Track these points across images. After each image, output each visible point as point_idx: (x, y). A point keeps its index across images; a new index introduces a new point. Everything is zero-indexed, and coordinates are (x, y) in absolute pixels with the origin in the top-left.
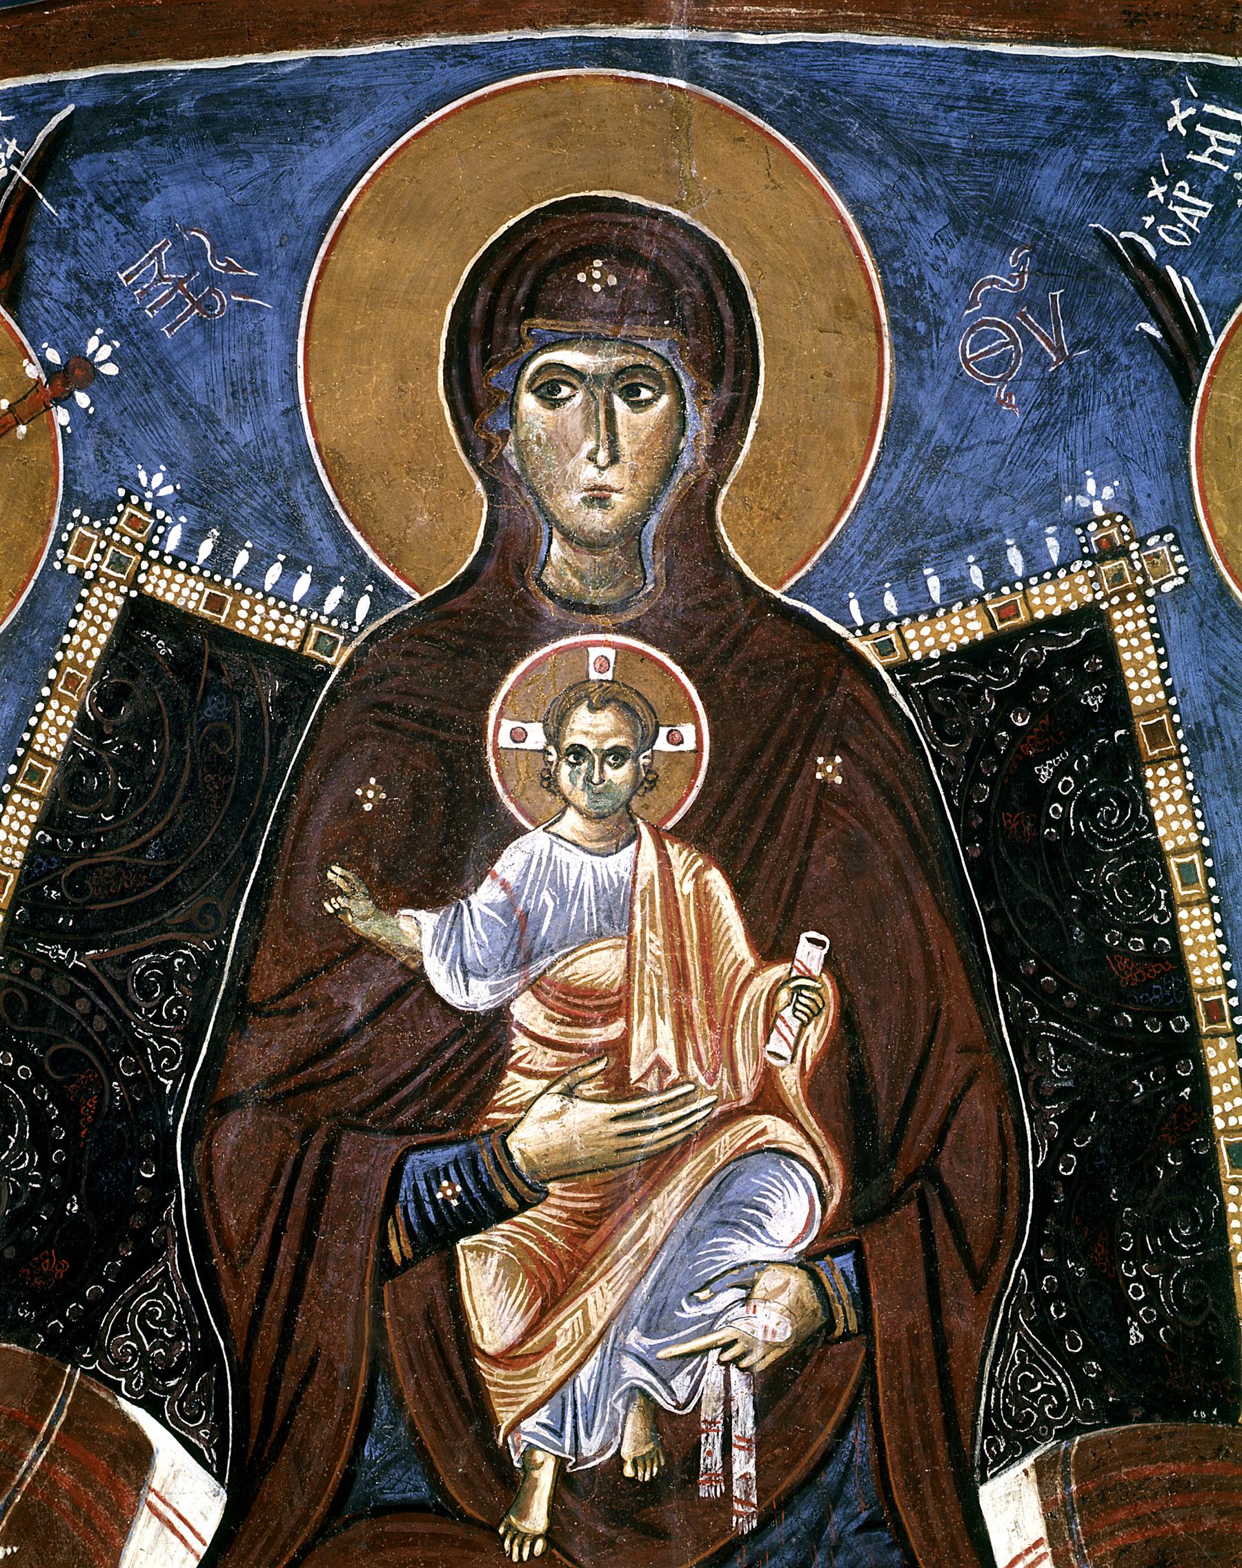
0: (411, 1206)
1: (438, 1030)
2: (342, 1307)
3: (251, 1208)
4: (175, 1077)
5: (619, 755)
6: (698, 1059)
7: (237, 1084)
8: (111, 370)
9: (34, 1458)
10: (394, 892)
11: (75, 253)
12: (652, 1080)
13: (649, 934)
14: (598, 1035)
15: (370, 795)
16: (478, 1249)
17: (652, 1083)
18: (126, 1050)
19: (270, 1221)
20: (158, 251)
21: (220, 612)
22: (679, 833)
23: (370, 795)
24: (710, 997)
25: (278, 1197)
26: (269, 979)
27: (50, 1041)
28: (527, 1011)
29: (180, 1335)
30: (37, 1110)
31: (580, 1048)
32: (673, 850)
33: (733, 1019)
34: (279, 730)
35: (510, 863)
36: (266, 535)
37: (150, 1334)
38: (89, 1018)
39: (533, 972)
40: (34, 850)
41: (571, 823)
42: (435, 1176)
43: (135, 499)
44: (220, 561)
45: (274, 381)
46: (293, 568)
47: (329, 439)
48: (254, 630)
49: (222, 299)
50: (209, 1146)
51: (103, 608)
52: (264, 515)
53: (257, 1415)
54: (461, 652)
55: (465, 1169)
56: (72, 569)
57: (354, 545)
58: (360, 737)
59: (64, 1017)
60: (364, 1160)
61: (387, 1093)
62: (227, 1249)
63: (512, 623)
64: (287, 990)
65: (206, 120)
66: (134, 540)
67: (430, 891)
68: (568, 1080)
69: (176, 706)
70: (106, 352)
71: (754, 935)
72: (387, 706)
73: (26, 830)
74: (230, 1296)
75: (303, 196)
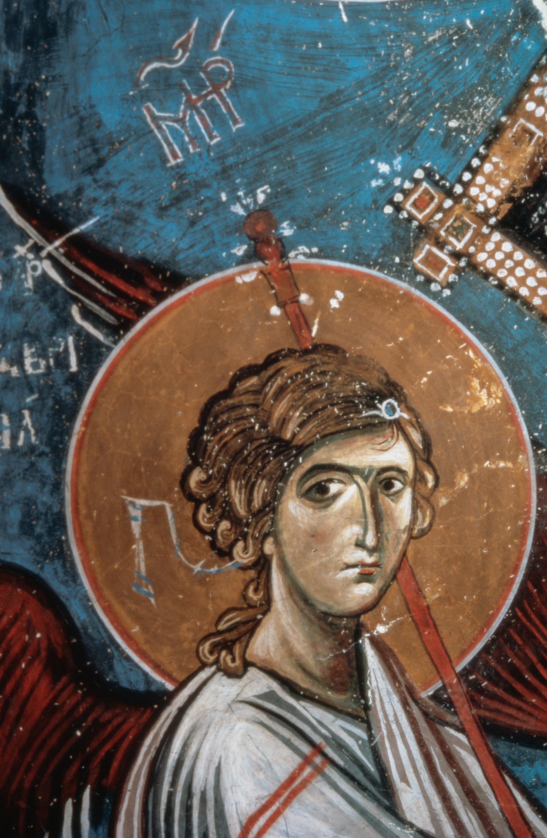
11: (140, 205)
20: (155, 119)
21: (532, 134)
43: (398, 197)
49: (215, 61)
51: (499, 256)
56: (452, 278)
65: (31, 39)
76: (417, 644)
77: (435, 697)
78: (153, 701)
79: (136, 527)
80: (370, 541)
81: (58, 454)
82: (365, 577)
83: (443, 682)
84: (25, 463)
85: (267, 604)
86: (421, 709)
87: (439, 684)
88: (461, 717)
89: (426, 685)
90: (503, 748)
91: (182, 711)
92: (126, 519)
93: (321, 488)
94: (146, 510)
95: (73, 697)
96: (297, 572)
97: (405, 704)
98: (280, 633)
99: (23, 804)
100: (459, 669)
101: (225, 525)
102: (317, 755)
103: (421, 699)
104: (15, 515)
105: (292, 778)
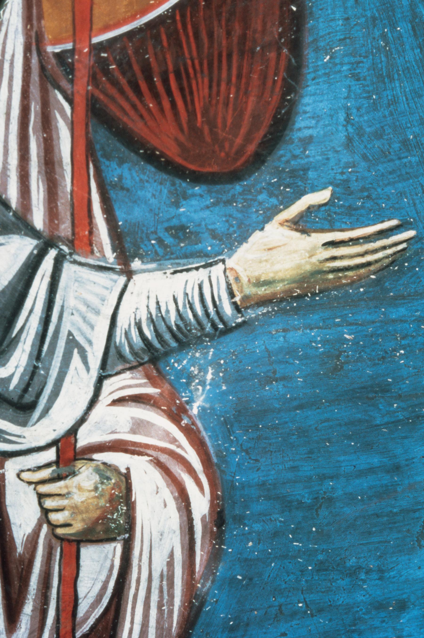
77: (59, 56)
83: (74, 46)
86: (40, 62)
87: (69, 46)
88: (76, 88)
89: (56, 42)
90: (102, 136)
97: (27, 49)
100: (95, 40)
103: (45, 52)
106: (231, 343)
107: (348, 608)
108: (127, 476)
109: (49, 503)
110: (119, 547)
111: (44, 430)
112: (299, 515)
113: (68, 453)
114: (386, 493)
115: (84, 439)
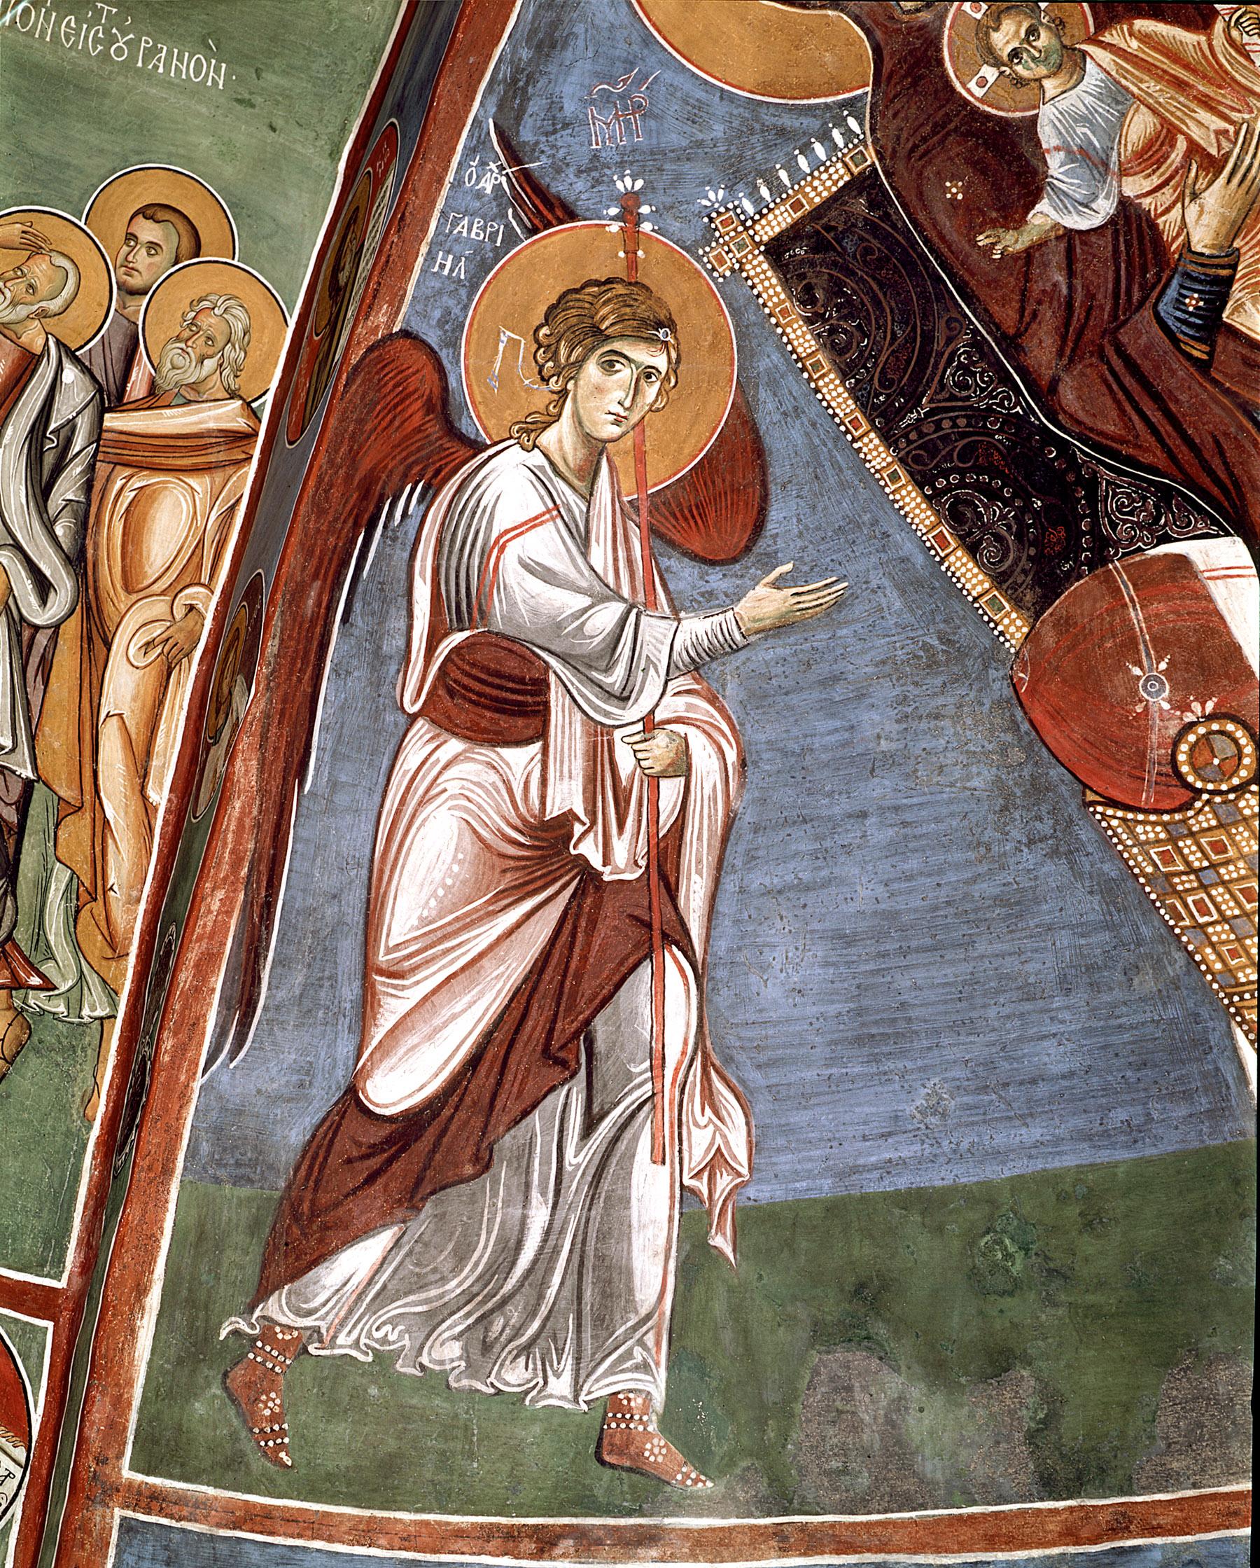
0: (1184, 328)
1: (1104, 245)
2: (1203, 405)
3: (1114, 414)
4: (1018, 403)
5: (1032, 31)
6: (1233, 109)
7: (1047, 374)
8: (639, 184)
9: (1136, 616)
10: (1014, 215)
12: (1225, 143)
13: (1143, 86)
14: (1177, 156)
15: (955, 190)
16: (1235, 310)
17: (1225, 143)
18: (985, 419)
19: (1128, 408)
22: (1101, 27)
23: (955, 190)
24: (1204, 77)
25: (1120, 395)
26: (1008, 316)
27: (950, 454)
28: (1133, 186)
29: (1144, 499)
30: (977, 486)
31: (1176, 171)
32: (1107, 38)
33: (1226, 72)
34: (886, 217)
35: (1047, 136)
36: (779, 153)
37: (1131, 513)
38: (955, 425)
39: (1114, 166)
40: (852, 391)
41: (1050, 86)
42: (1179, 303)
43: (714, 215)
44: (777, 188)
45: (700, 94)
46: (806, 149)
47: (750, 82)
48: (825, 194)
49: (640, 96)
50: (1065, 412)
52: (768, 147)
53: (1215, 491)
54: (914, 84)
55: (1188, 284)
56: (728, 273)
57: (817, 106)
58: (920, 174)
59: (945, 439)
60: (1141, 333)
61: (1116, 295)
62: (1122, 441)
63: (918, 43)
64: (1022, 310)
66: (735, 230)
67: (1030, 193)
68: (1187, 192)
69: (835, 263)
70: (628, 181)
71: (1188, 25)
72: (915, 147)
73: (841, 390)
74: (1146, 458)
75: (611, 16)
76: (632, 470)
78: (477, 447)
79: (501, 347)
80: (627, 404)
81: (473, 288)
82: (617, 423)
84: (452, 287)
85: (559, 415)
90: (658, 544)
91: (490, 458)
92: (498, 340)
93: (611, 364)
94: (510, 339)
95: (434, 429)
96: (580, 405)
98: (560, 437)
99: (384, 476)
101: (550, 364)
102: (556, 509)
104: (437, 314)
105: (536, 518)
106: (742, 655)
107: (830, 818)
108: (686, 739)
109: (640, 755)
110: (683, 779)
111: (636, 711)
112: (793, 760)
113: (650, 724)
114: (845, 744)
115: (659, 716)
